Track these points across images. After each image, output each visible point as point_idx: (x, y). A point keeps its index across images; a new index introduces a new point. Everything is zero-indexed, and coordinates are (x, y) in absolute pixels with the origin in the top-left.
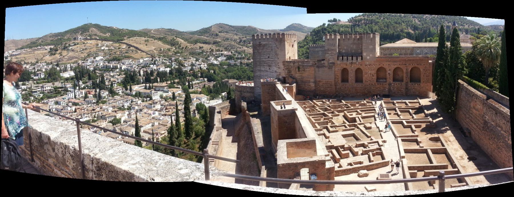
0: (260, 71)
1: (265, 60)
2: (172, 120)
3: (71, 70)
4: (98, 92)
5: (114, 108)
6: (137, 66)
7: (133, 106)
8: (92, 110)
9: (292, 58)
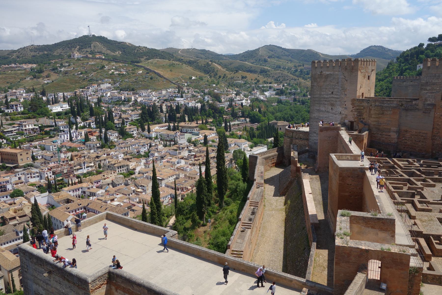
0: (319, 111)
1: (327, 96)
2: (200, 171)
3: (64, 100)
4: (104, 132)
5: (126, 155)
6: (158, 98)
7: (152, 152)
8: (95, 158)
9: (366, 95)
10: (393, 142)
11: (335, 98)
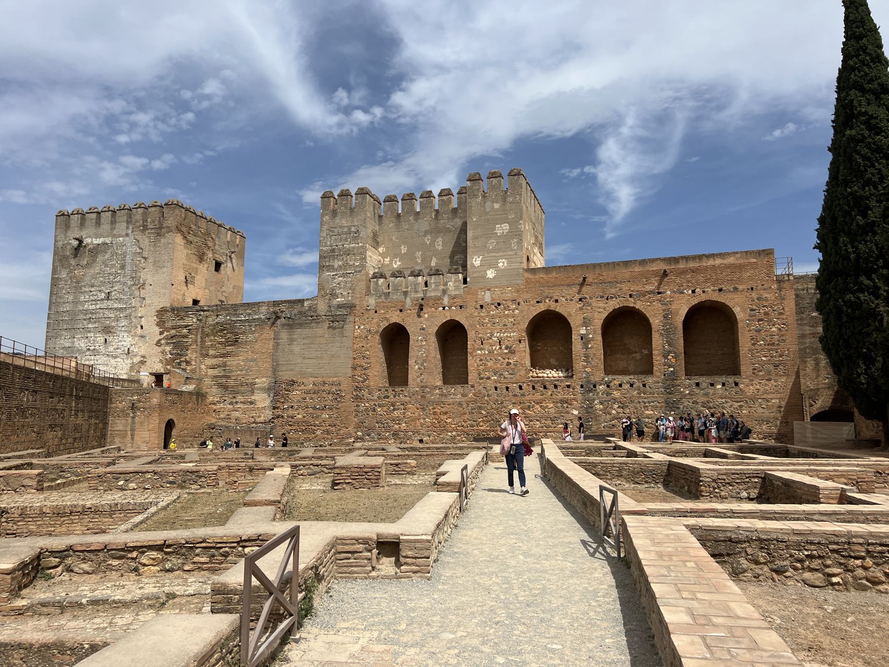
10: (262, 419)
11: (116, 309)
